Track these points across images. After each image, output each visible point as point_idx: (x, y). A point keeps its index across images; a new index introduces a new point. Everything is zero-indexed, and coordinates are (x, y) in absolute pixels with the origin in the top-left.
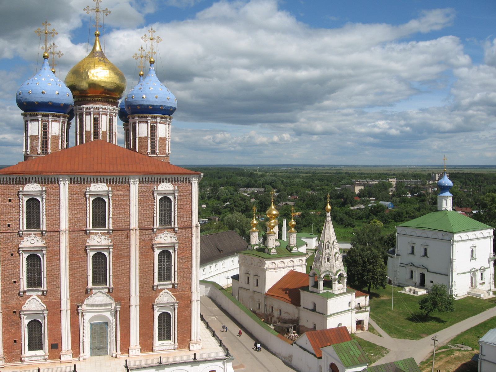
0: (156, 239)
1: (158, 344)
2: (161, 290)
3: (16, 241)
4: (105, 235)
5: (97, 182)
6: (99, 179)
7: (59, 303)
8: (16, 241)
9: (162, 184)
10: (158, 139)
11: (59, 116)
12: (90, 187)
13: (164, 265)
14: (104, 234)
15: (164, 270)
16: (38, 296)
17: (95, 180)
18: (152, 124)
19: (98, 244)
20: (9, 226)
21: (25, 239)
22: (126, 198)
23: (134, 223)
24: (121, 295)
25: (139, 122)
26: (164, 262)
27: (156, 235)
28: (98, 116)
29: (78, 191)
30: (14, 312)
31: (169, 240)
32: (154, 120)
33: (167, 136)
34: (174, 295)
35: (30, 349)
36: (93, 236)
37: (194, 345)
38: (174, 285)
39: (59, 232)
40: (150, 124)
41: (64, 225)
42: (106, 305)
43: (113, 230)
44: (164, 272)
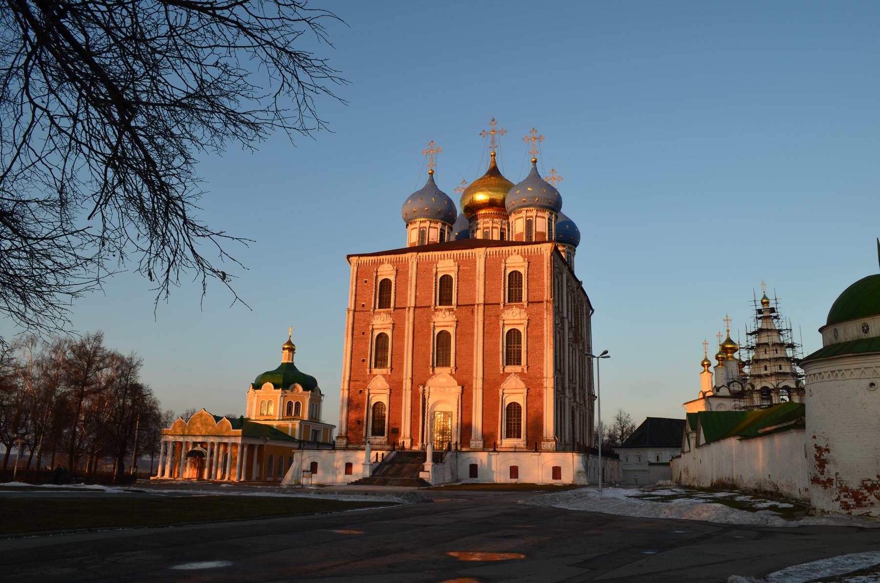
0: (502, 315)
1: (507, 443)
2: (509, 374)
3: (368, 319)
4: (449, 311)
5: (444, 259)
6: (446, 256)
7: (401, 383)
8: (368, 319)
9: (511, 257)
10: (534, 233)
11: (437, 223)
12: (438, 265)
13: (514, 347)
14: (450, 310)
15: (514, 353)
16: (384, 376)
17: (442, 257)
18: (528, 219)
19: (442, 320)
20: (363, 305)
21: (376, 316)
22: (472, 273)
23: (480, 299)
24: (464, 377)
25: (516, 219)
26: (514, 344)
27: (503, 311)
28: (488, 230)
29: (426, 268)
30: (361, 391)
31: (517, 317)
32: (529, 214)
33: (547, 231)
34: (523, 381)
35: (373, 434)
36: (437, 312)
37: (546, 443)
38: (523, 369)
39: (405, 308)
40: (526, 218)
41: (411, 302)
42: (449, 387)
43: (458, 306)
44: (514, 356)
